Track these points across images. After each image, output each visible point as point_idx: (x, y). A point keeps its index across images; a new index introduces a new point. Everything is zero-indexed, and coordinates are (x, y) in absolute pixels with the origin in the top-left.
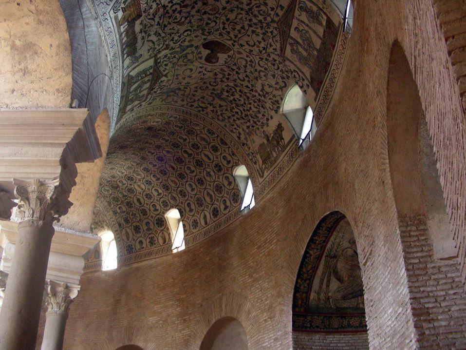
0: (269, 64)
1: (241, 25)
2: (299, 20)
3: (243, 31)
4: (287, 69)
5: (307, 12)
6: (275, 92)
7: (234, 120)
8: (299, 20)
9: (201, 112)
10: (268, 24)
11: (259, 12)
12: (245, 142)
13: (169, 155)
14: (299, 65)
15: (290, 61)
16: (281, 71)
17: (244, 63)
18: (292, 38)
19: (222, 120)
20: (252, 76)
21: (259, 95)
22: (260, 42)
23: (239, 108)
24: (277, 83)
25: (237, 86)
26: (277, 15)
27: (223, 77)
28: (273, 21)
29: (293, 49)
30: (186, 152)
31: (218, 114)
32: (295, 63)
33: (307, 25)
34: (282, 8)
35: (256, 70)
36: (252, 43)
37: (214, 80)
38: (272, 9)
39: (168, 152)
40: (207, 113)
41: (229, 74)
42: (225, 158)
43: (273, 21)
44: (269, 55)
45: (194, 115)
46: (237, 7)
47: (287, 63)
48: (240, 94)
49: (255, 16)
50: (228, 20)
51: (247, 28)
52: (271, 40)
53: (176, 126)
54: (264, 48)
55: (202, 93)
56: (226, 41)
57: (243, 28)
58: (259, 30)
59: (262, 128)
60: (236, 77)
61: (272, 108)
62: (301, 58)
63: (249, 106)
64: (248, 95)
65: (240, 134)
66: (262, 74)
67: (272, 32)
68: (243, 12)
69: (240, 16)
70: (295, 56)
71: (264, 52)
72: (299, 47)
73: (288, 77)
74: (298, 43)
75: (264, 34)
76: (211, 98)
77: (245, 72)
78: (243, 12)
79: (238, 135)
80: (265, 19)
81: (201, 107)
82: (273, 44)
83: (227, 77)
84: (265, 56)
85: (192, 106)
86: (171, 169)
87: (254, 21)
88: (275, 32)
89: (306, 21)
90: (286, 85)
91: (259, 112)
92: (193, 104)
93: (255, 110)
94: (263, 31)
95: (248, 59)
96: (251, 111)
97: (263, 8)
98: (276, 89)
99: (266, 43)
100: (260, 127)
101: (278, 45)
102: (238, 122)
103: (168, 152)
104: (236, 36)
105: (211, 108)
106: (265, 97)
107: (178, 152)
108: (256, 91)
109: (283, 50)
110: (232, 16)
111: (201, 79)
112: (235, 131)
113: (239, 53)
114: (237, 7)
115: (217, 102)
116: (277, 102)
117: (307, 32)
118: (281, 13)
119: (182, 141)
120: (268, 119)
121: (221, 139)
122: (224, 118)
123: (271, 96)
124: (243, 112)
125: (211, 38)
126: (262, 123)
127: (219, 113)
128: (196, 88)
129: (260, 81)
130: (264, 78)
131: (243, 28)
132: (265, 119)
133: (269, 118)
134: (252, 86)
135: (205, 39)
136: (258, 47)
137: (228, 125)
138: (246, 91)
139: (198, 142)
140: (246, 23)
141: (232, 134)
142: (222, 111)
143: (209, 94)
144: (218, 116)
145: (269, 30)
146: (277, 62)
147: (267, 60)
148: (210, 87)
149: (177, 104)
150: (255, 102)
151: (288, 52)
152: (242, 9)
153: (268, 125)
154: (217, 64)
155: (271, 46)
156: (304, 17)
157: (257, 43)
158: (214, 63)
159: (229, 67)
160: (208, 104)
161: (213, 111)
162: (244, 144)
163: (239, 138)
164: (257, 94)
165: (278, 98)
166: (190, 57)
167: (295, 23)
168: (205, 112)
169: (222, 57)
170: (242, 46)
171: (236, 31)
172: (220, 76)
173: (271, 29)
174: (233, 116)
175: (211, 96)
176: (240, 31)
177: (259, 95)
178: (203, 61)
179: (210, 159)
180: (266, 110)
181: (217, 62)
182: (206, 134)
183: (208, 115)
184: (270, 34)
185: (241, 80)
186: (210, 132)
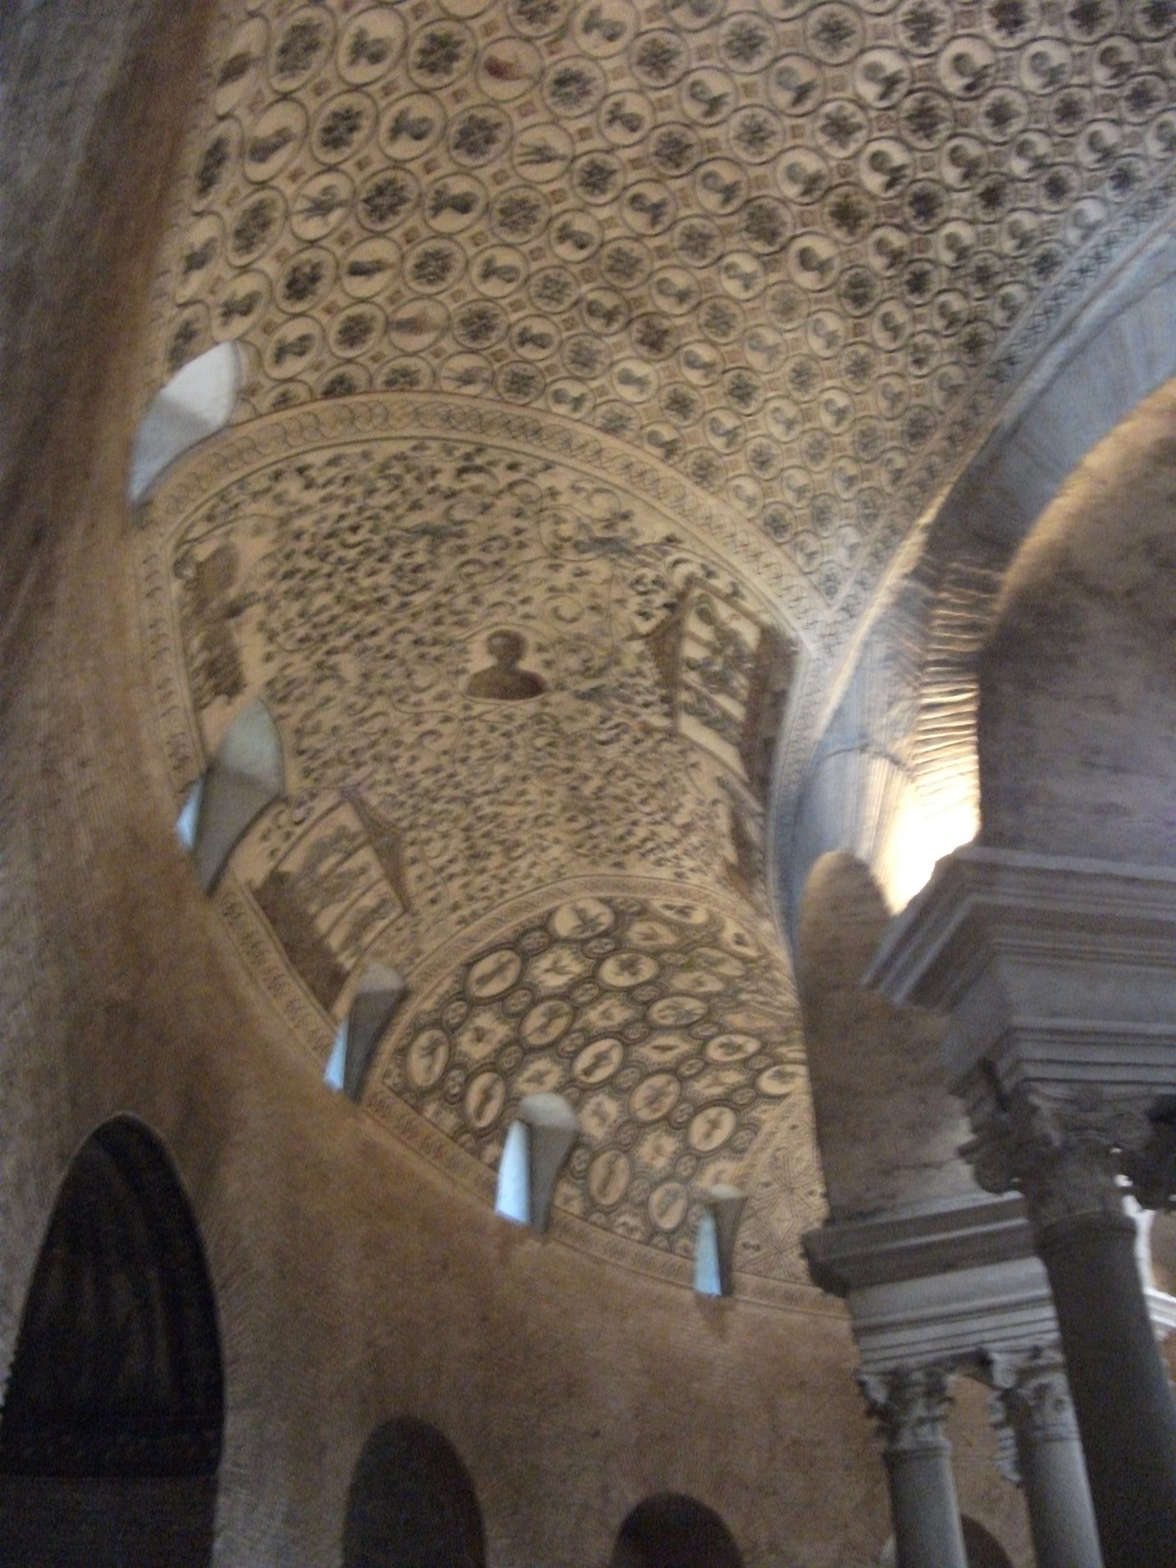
4: (324, 784)
6: (303, 708)
7: (348, 501)
9: (469, 448)
12: (279, 488)
13: (531, 138)
14: (314, 836)
15: (332, 809)
17: (421, 682)
18: (361, 846)
19: (384, 466)
20: (381, 668)
23: (358, 549)
25: (404, 605)
26: (412, 843)
27: (451, 603)
30: (463, 205)
31: (414, 474)
34: (414, 861)
35: (380, 692)
37: (477, 579)
39: (543, 155)
40: (449, 451)
41: (438, 622)
42: (302, 346)
45: (491, 424)
47: (330, 799)
48: (381, 593)
50: (507, 758)
52: (391, 789)
53: (540, 341)
54: (393, 760)
55: (495, 526)
56: (491, 707)
58: (427, 782)
60: (417, 627)
62: (321, 850)
63: (339, 587)
64: (357, 616)
65: (309, 485)
66: (361, 702)
75: (414, 786)
76: (458, 514)
77: (402, 663)
79: (313, 473)
81: (479, 469)
83: (443, 611)
84: (383, 747)
85: (513, 467)
86: (504, 52)
87: (448, 792)
92: (515, 476)
95: (414, 698)
97: (443, 827)
98: (308, 715)
100: (270, 584)
101: (373, 800)
102: (336, 509)
103: (543, 155)
105: (445, 481)
107: (498, 179)
109: (360, 806)
110: (500, 770)
111: (513, 578)
112: (331, 472)
113: (441, 697)
115: (432, 515)
118: (410, 852)
119: (505, 258)
120: (272, 637)
121: (350, 390)
122: (385, 477)
124: (342, 553)
125: (528, 707)
127: (409, 481)
128: (522, 546)
130: (352, 699)
134: (365, 650)
135: (545, 704)
137: (363, 467)
138: (371, 619)
139: (429, 297)
140: (462, 771)
141: (327, 455)
142: (404, 493)
143: (470, 529)
144: (409, 470)
148: (472, 554)
149: (573, 476)
152: (487, 793)
153: (262, 627)
154: (487, 634)
158: (495, 635)
159: (451, 643)
160: (461, 491)
161: (434, 473)
162: (277, 476)
163: (301, 471)
166: (573, 662)
167: (375, 872)
168: (457, 454)
169: (480, 661)
170: (447, 719)
172: (462, 602)
174: (361, 510)
175: (462, 522)
178: (531, 639)
179: (357, 270)
181: (490, 639)
182: (415, 354)
183: (444, 446)
185: (401, 631)
186: (402, 380)
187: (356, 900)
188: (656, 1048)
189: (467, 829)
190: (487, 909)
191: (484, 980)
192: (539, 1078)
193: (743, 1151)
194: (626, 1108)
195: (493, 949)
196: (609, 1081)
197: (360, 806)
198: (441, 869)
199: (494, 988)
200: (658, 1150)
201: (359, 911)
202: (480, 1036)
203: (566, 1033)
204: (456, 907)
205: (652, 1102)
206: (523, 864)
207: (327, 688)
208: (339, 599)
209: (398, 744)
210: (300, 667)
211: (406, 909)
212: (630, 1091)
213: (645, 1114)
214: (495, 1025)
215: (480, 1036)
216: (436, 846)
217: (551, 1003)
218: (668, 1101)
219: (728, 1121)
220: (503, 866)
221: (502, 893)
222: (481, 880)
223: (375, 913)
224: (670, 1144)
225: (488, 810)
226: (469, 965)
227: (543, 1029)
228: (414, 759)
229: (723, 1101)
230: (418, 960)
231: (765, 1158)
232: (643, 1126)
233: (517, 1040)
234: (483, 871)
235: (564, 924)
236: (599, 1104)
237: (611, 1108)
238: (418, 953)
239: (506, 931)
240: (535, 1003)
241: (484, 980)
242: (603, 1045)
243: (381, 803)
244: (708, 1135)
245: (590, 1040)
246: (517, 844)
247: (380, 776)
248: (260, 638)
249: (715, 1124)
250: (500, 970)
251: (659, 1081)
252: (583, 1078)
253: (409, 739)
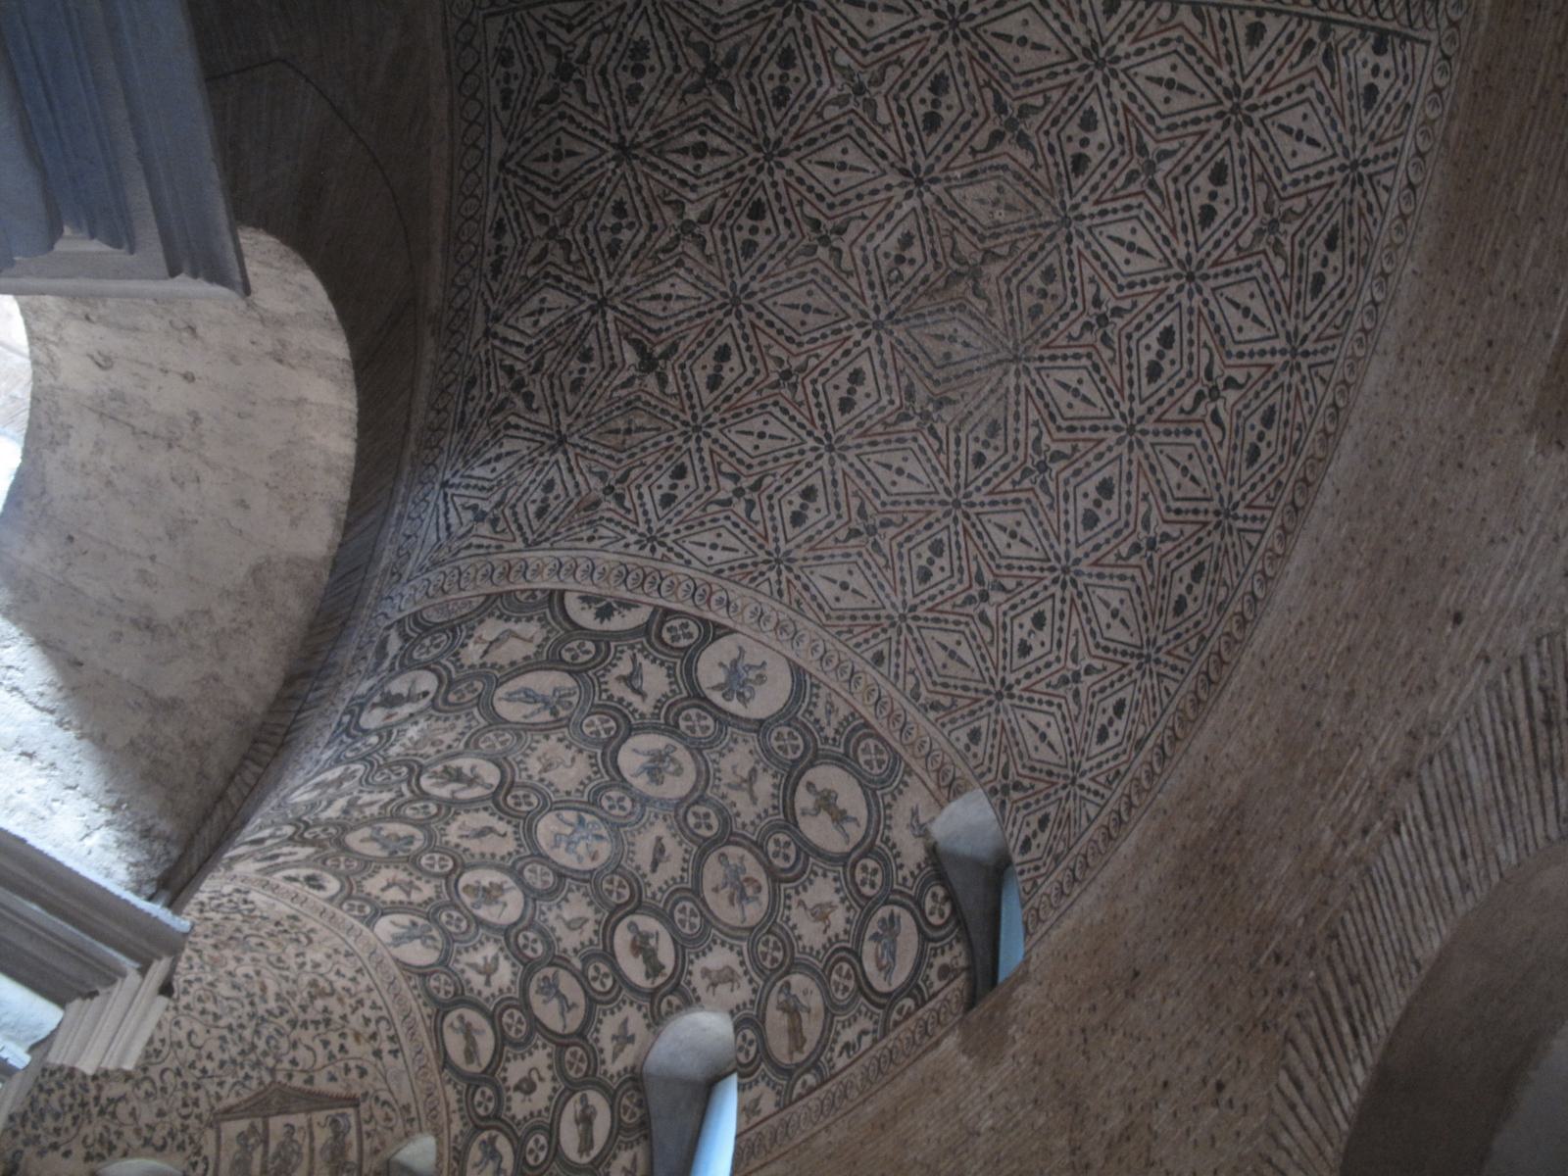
0: (180, 1095)
1: (219, 1012)
2: (310, 1126)
3: (210, 1018)
5: (336, 1137)
6: (128, 1133)
8: (310, 1126)
10: (257, 1064)
11: (270, 1037)
15: (218, 1138)
16: (185, 1128)
21: (97, 1099)
22: (210, 1057)
24: (151, 1128)
26: (290, 1076)
28: (272, 1071)
29: (246, 1139)
32: (223, 1154)
33: (312, 1150)
34: (310, 1081)
36: (198, 1042)
38: (294, 1062)
43: (272, 1071)
44: (197, 1087)
46: (250, 995)
47: (210, 1134)
49: (257, 1032)
51: (223, 1023)
52: (230, 1080)
54: (204, 1071)
57: (216, 1017)
58: (234, 1050)
59: (26, 1144)
61: (90, 1141)
63: (53, 1085)
66: (146, 1086)
67: (247, 1077)
68: (248, 1009)
69: (235, 1004)
70: (236, 1147)
71: (197, 1073)
72: (260, 1149)
73: (181, 1147)
74: (266, 1142)
75: (234, 1062)
78: (248, 1009)
80: (265, 1054)
82: (227, 1086)
84: (190, 1080)
88: (254, 1084)
89: (318, 1144)
90: (163, 1147)
91: (57, 1116)
93: (56, 1105)
94: (239, 1059)
96: (43, 1096)
97: (284, 1044)
98: (138, 1132)
99: (219, 1072)
101: (232, 1100)
104: (188, 1007)
106: (102, 1112)
108: (100, 1088)
109: (229, 1113)
114: (250, 995)
116: (112, 1148)
117: (299, 1154)
118: (298, 1081)
120: (55, 1147)
123: (113, 1128)
126: (37, 1137)
129: (127, 1087)
130: (141, 1093)
131: (216, 1017)
132: (53, 1139)
133: (63, 1149)
136: (199, 1057)
145: (247, 1069)
146: (196, 1111)
147: (185, 1085)
150: (73, 1094)
151: (233, 1128)
152: (252, 1004)
153: (42, 1153)
155: (221, 1084)
156: (323, 1136)
157: (204, 1053)
164: (93, 1092)
165: (121, 1146)
167: (299, 1120)
170: (177, 1023)
171: (199, 1006)
173: (254, 1074)
176: (203, 1012)
177: (97, 1099)
180: (73, 1131)
184: (241, 1074)
187: (312, 1150)
188: (655, 865)
189: (293, 1023)
190: (390, 1023)
191: (471, 1054)
192: (624, 1038)
193: (896, 757)
194: (732, 934)
195: (437, 1033)
196: (681, 944)
197: (229, 1113)
198: (331, 1056)
199: (486, 1043)
200: (821, 914)
201: (322, 1151)
202: (527, 1087)
203: (581, 977)
204: (377, 1053)
205: (740, 896)
206: (339, 983)
207: (123, 1110)
208: (61, 1086)
209: (192, 1066)
210: (92, 1130)
211: (353, 1102)
212: (708, 919)
213: (754, 912)
214: (529, 1062)
215: (527, 1087)
216: (302, 1054)
217: (533, 987)
218: (753, 869)
219: (827, 776)
220: (341, 1000)
221: (374, 1006)
222: (355, 1021)
223: (339, 1134)
224: (823, 890)
225: (272, 1004)
226: (446, 1062)
227: (567, 1007)
228: (210, 1057)
229: (791, 777)
230: (414, 1114)
231: (924, 725)
232: (770, 923)
233: (561, 1042)
234: (344, 1017)
235: (419, 954)
236: (706, 973)
237: (719, 958)
238: (406, 1108)
239: (421, 1012)
240: (525, 1006)
241: (471, 1054)
242: (622, 938)
243: (238, 1094)
244: (840, 818)
245: (609, 956)
246: (313, 984)
247: (213, 1089)
248: (51, 1155)
249: (825, 800)
250: (468, 1031)
251: (713, 872)
252: (660, 980)
253: (192, 1055)
